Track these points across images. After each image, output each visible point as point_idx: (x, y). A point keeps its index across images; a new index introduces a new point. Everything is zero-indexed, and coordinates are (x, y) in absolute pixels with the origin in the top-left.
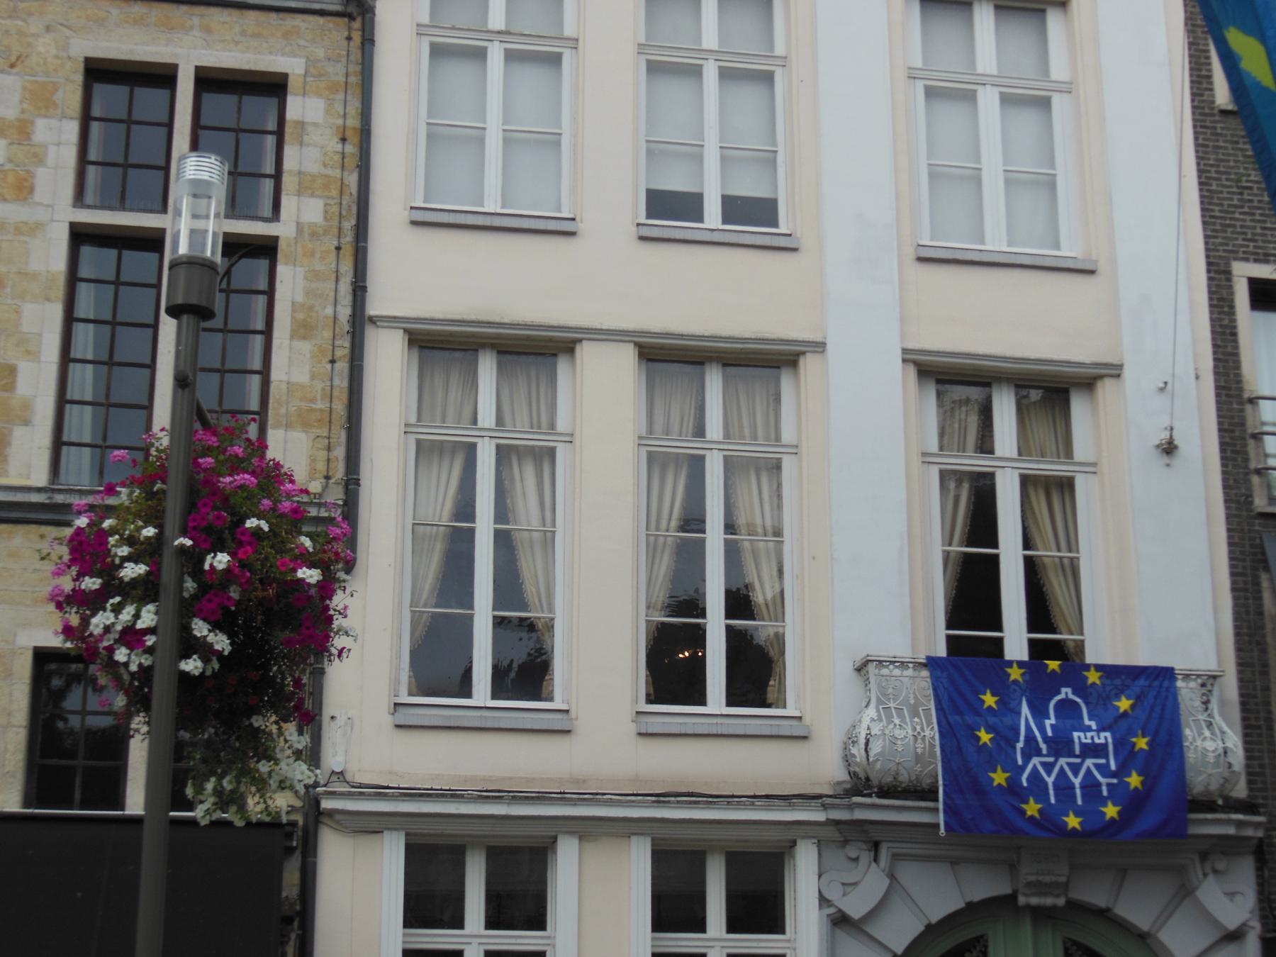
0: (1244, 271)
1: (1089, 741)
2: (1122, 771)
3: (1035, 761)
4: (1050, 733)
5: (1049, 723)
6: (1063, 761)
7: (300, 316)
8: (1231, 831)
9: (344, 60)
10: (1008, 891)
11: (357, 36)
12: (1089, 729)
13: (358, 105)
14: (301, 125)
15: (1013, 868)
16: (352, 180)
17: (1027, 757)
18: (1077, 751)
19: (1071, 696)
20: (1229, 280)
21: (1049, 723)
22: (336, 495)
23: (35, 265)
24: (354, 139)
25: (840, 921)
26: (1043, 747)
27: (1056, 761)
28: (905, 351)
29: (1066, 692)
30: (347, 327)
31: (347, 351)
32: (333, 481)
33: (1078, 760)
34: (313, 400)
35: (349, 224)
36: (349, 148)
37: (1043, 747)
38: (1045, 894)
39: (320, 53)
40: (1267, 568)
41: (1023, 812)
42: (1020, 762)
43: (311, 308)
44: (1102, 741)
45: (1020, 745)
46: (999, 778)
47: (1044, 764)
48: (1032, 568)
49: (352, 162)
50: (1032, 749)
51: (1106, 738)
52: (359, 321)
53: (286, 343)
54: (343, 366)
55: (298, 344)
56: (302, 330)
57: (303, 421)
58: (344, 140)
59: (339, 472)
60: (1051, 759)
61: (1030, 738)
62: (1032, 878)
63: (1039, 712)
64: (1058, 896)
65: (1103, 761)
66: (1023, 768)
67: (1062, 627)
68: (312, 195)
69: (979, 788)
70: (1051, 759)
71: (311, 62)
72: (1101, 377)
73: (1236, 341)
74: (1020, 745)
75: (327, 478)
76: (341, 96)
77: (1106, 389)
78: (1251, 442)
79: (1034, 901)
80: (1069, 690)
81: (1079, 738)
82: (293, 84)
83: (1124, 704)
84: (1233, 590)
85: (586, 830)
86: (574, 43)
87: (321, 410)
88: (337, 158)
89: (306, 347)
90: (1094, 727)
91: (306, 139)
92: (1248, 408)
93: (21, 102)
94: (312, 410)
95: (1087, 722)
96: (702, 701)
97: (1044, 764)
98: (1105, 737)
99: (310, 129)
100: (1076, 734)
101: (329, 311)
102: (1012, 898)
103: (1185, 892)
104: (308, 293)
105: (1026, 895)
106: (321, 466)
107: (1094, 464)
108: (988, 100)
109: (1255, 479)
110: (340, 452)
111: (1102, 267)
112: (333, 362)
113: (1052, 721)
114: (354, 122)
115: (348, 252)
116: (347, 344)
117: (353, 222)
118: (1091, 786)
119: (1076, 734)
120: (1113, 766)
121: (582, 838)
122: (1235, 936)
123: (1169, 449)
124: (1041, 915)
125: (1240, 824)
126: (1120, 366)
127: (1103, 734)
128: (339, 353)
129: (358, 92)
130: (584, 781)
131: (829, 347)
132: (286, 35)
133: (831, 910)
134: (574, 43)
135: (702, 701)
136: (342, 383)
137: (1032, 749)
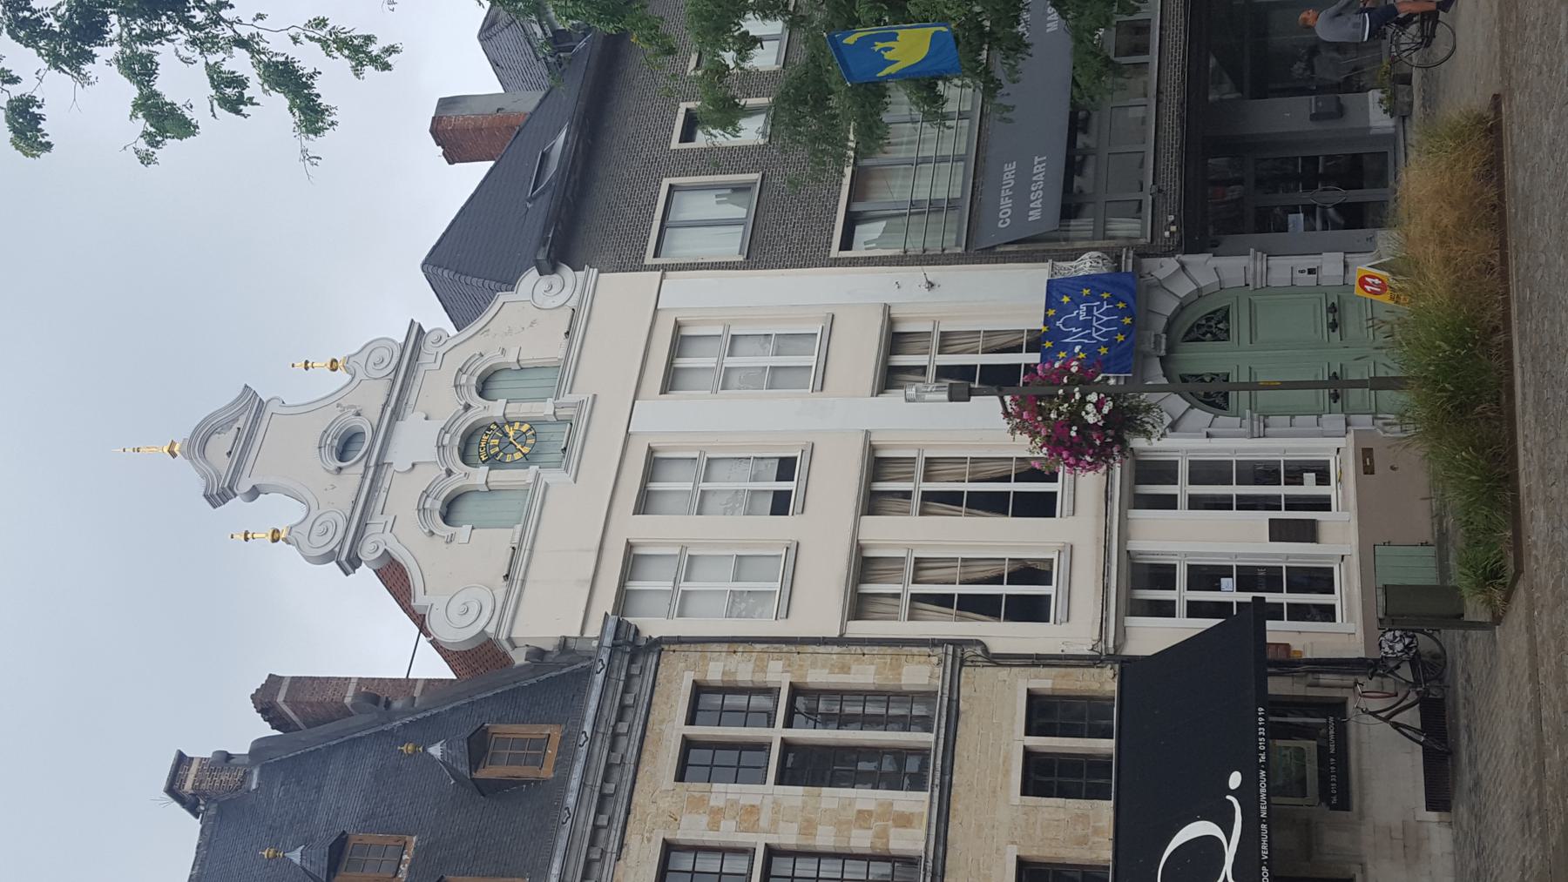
0: (835, 252)
2: (1102, 300)
3: (1094, 335)
4: (1080, 329)
5: (1074, 330)
6: (1095, 324)
7: (837, 670)
8: (1130, 261)
9: (687, 653)
10: (1158, 359)
11: (673, 647)
12: (1078, 313)
13: (715, 645)
14: (723, 673)
15: (1146, 356)
16: (758, 647)
17: (1093, 339)
20: (840, 259)
21: (1074, 330)
22: (939, 650)
23: (798, 802)
24: (735, 647)
25: (1173, 427)
26: (1087, 332)
28: (872, 396)
30: (845, 648)
31: (858, 648)
32: (931, 653)
33: (1094, 318)
34: (886, 663)
35: (784, 648)
36: (740, 649)
37: (1087, 332)
38: (1160, 342)
39: (682, 665)
40: (994, 247)
41: (1122, 341)
43: (832, 665)
44: (1085, 308)
45: (1086, 341)
46: (1103, 351)
47: (1096, 332)
48: (986, 351)
49: (748, 647)
50: (1089, 336)
52: (841, 641)
53: (852, 676)
54: (866, 650)
55: (853, 671)
56: (845, 669)
57: (897, 668)
58: (735, 652)
59: (927, 650)
61: (1082, 337)
62: (1152, 346)
63: (1068, 335)
64: (1161, 337)
65: (1095, 308)
66: (1098, 340)
67: (1020, 341)
68: (767, 666)
69: (1107, 359)
70: (1094, 329)
71: (687, 668)
72: (889, 315)
73: (873, 257)
74: (1086, 341)
75: (929, 656)
76: (709, 654)
77: (895, 313)
78: (927, 253)
79: (1163, 347)
82: (699, 677)
83: (1066, 299)
84: (1005, 263)
85: (1124, 537)
86: (684, 548)
87: (891, 659)
88: (745, 654)
89: (854, 668)
91: (733, 670)
92: (909, 253)
93: (700, 814)
94: (891, 664)
95: (1075, 314)
96: (1055, 493)
97: (1096, 332)
98: (1083, 307)
99: (727, 668)
100: (1081, 318)
101: (834, 656)
102: (1162, 359)
103: (1160, 285)
104: (823, 667)
105: (1160, 350)
106: (923, 659)
107: (935, 322)
108: (730, 362)
109: (946, 252)
110: (915, 650)
111: (831, 311)
112: (864, 654)
114: (725, 647)
115: (800, 648)
116: (854, 648)
117: (784, 646)
119: (1081, 318)
120: (1098, 303)
121: (1128, 538)
122: (1183, 267)
123: (931, 285)
124: (1170, 349)
125: (1127, 257)
126: (885, 304)
128: (859, 651)
129: (707, 645)
130: (1098, 538)
131: (869, 428)
132: (669, 682)
133: (1167, 430)
134: (684, 548)
135: (1054, 494)
136: (876, 649)
137: (1089, 336)
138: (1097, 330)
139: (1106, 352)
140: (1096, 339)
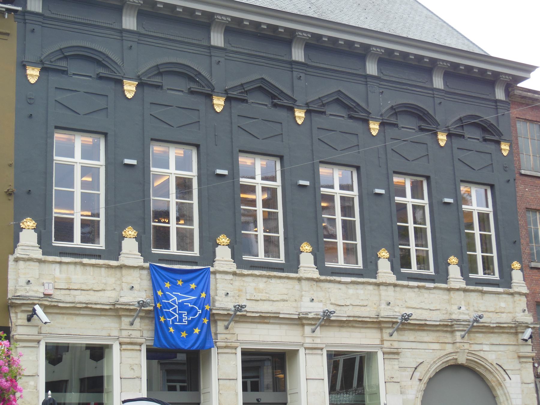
1: (184, 317)
2: (175, 327)
3: (176, 298)
6: (177, 306)
12: (188, 318)
18: (180, 312)
19: (198, 313)
27: (177, 305)
29: (200, 311)
33: (177, 313)
37: (180, 301)
42: (173, 293)
44: (184, 321)
51: (185, 323)
60: (177, 304)
70: (177, 304)
80: (201, 312)
81: (185, 313)
90: (188, 319)
95: (190, 317)
113: (190, 306)
118: (170, 315)
127: (187, 322)
138: (174, 301)
139: (194, 288)
140: (173, 295)
